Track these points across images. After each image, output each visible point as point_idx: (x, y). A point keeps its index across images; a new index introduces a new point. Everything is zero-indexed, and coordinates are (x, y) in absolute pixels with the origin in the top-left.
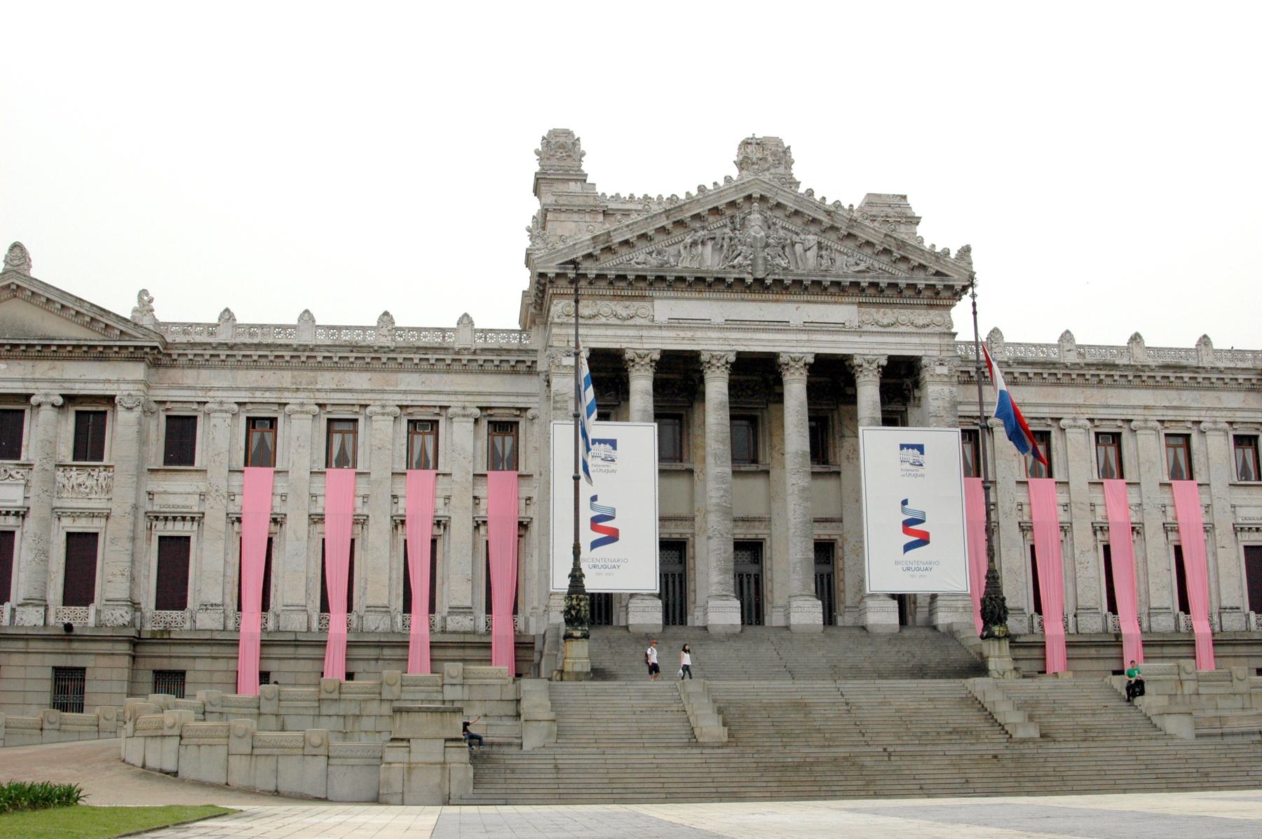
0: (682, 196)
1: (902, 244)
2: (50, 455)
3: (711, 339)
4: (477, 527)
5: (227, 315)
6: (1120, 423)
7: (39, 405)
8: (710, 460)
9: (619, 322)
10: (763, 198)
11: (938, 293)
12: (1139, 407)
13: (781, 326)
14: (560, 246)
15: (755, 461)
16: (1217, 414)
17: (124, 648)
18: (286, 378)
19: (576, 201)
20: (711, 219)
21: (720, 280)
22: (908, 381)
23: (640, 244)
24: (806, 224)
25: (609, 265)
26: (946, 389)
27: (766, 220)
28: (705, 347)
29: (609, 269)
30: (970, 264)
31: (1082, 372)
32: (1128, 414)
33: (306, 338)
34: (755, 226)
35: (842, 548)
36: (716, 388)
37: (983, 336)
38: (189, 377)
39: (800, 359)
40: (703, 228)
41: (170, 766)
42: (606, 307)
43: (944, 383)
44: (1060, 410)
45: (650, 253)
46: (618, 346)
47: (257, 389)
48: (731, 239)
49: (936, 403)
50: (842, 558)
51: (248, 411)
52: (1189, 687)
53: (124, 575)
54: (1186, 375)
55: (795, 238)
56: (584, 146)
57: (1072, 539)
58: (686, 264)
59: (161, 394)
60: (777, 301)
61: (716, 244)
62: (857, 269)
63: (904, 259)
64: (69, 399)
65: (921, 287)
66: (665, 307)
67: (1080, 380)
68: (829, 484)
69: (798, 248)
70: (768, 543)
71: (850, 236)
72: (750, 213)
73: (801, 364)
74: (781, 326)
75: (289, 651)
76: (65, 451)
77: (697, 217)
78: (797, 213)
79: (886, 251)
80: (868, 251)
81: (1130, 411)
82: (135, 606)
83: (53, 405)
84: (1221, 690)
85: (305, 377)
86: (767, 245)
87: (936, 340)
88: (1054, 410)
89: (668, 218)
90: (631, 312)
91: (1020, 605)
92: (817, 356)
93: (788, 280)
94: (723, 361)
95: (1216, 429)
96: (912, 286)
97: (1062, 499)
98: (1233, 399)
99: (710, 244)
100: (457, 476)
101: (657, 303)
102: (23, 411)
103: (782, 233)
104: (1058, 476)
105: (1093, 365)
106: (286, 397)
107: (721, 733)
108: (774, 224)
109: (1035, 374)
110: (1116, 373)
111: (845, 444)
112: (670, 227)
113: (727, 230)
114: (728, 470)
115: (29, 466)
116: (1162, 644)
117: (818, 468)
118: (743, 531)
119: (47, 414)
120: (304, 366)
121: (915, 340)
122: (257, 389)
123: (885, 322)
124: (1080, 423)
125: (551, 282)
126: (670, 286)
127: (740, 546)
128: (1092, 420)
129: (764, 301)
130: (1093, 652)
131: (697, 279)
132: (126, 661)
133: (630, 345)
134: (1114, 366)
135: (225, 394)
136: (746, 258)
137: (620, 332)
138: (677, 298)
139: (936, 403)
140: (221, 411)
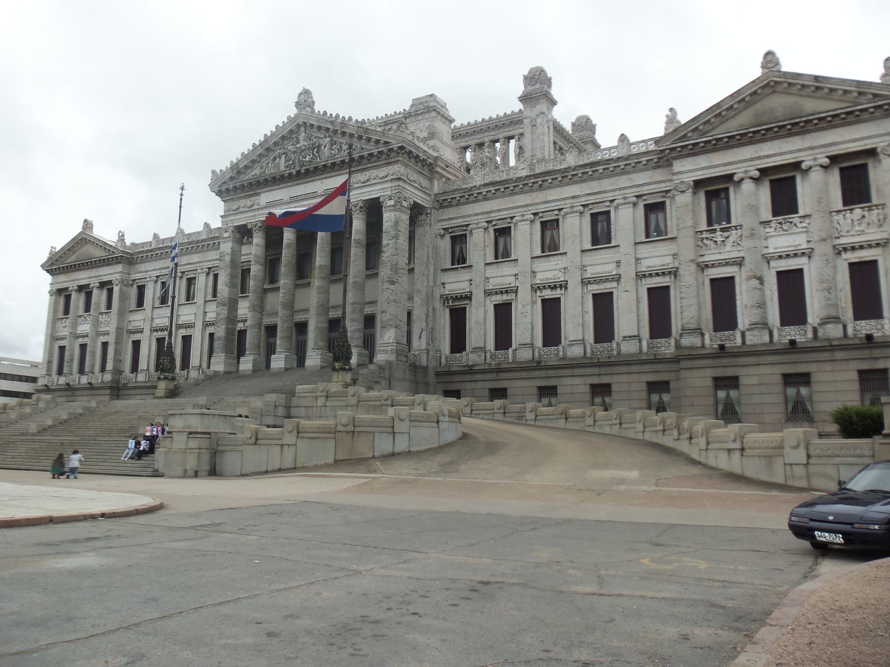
0: (269, 134)
5: (156, 236)
6: (557, 212)
10: (305, 123)
12: (568, 198)
16: (627, 191)
21: (282, 176)
23: (256, 166)
26: (393, 214)
36: (289, 235)
52: (321, 401)
54: (600, 168)
58: (270, 171)
59: (133, 277)
66: (265, 197)
67: (526, 188)
71: (344, 133)
77: (276, 144)
78: (319, 128)
81: (562, 203)
84: (340, 404)
87: (389, 185)
88: (510, 212)
91: (482, 345)
95: (626, 203)
98: (640, 178)
110: (549, 179)
116: (572, 366)
121: (378, 187)
130: (524, 374)
139: (389, 224)
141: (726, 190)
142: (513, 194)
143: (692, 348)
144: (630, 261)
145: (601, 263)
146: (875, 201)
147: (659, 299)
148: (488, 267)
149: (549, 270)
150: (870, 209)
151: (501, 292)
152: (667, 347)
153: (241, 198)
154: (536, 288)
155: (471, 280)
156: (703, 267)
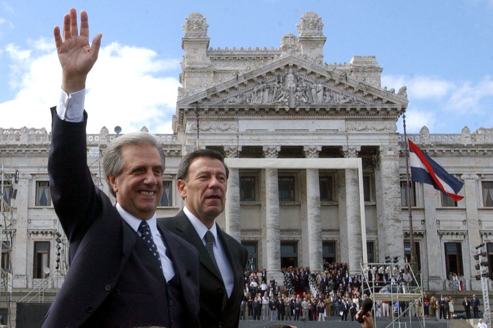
1: (368, 88)
3: (269, 140)
8: (268, 202)
9: (221, 132)
10: (294, 66)
11: (388, 112)
13: (304, 132)
14: (191, 95)
20: (267, 77)
22: (375, 157)
24: (318, 78)
25: (215, 102)
26: (393, 163)
27: (296, 77)
28: (265, 144)
29: (215, 106)
30: (406, 96)
31: (474, 149)
35: (339, 244)
39: (314, 149)
40: (263, 83)
42: (214, 125)
43: (392, 160)
44: (461, 170)
45: (236, 97)
46: (220, 144)
47: (41, 167)
48: (278, 88)
49: (387, 170)
50: (339, 250)
51: (37, 178)
55: (313, 87)
57: (468, 239)
60: (302, 119)
61: (270, 90)
62: (344, 101)
63: (370, 95)
65: (379, 109)
66: (245, 124)
67: (473, 153)
69: (313, 91)
70: (300, 242)
72: (288, 74)
73: (315, 151)
74: (304, 132)
77: (261, 77)
78: (312, 73)
79: (360, 91)
80: (351, 91)
86: (297, 91)
87: (387, 137)
88: (458, 170)
89: (245, 78)
90: (227, 127)
91: (438, 275)
93: (308, 108)
94: (274, 151)
96: (376, 109)
97: (463, 218)
99: (267, 90)
101: (240, 122)
103: (304, 84)
105: (480, 145)
108: (301, 79)
109: (446, 151)
111: (341, 191)
112: (246, 83)
113: (276, 83)
117: (326, 203)
118: (288, 236)
121: (376, 137)
122: (41, 167)
123: (360, 128)
124: (473, 176)
125: (186, 113)
126: (246, 113)
127: (284, 243)
128: (479, 175)
129: (295, 119)
131: (260, 109)
133: (226, 144)
135: (25, 170)
136: (285, 98)
137: (221, 137)
138: (250, 119)
140: (23, 178)
142: (460, 155)
148: (438, 212)
151: (452, 234)
153: (212, 120)
155: (424, 221)
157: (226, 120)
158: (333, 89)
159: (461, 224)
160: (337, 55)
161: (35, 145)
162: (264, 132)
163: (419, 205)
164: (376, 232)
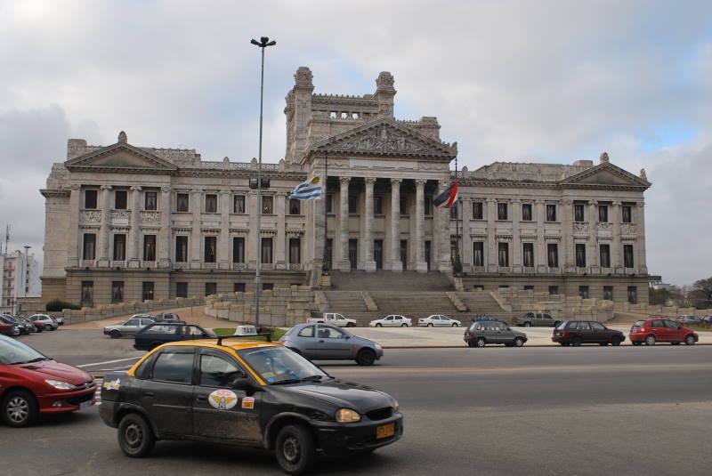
1: (434, 142)
2: (138, 208)
4: (286, 234)
7: (133, 190)
8: (367, 215)
10: (387, 125)
15: (381, 213)
17: (168, 275)
18: (219, 181)
19: (322, 119)
21: (371, 154)
25: (335, 148)
32: (510, 197)
33: (227, 168)
34: (384, 136)
36: (369, 190)
37: (460, 169)
38: (186, 180)
41: (226, 317)
53: (165, 250)
56: (313, 74)
58: (360, 148)
64: (144, 188)
66: (353, 162)
68: (405, 221)
71: (417, 138)
75: (223, 276)
76: (143, 206)
77: (365, 131)
79: (428, 144)
82: (169, 260)
83: (139, 191)
85: (226, 181)
87: (443, 175)
92: (404, 180)
98: (547, 192)
100: (280, 216)
102: (126, 192)
104: (484, 219)
106: (220, 188)
107: (375, 308)
114: (372, 218)
115: (130, 211)
119: (135, 194)
120: (226, 177)
130: (493, 279)
132: (168, 280)
134: (506, 180)
141: (582, 207)
142: (486, 186)
143: (572, 273)
144: (540, 230)
145: (528, 229)
146: (633, 222)
147: (553, 248)
149: (503, 229)
150: (632, 225)
152: (559, 271)
154: (497, 237)
156: (575, 238)
157: (342, 159)
158: (411, 141)
159: (484, 231)
160: (406, 109)
161: (206, 170)
162: (366, 168)
163: (460, 218)
164: (432, 235)
